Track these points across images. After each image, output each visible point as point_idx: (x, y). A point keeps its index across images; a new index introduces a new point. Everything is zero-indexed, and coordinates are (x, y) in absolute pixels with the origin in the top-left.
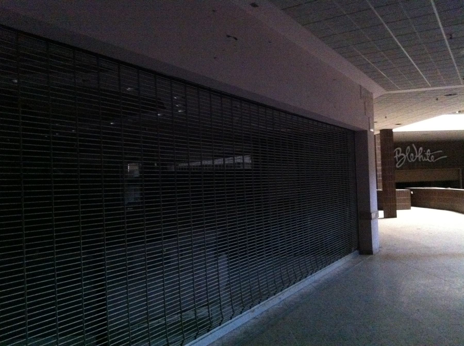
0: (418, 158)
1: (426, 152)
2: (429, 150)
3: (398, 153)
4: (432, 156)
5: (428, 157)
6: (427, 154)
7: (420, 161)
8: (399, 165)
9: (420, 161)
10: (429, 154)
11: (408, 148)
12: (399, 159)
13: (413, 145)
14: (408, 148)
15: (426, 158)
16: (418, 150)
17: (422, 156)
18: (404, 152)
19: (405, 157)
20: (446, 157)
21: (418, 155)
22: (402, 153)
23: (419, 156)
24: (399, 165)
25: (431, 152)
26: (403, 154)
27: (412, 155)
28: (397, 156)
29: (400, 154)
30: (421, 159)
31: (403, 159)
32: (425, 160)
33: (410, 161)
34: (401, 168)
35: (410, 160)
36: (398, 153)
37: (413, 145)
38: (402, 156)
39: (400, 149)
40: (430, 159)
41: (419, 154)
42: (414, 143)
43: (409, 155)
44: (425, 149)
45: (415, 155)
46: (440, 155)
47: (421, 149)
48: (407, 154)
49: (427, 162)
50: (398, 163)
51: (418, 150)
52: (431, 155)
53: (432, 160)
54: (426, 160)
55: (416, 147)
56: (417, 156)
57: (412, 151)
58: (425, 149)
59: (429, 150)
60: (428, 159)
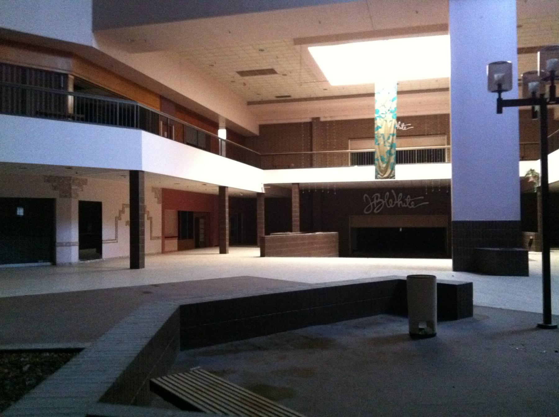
0: (397, 204)
1: (406, 198)
2: (409, 196)
4: (413, 203)
6: (407, 200)
7: (399, 206)
8: (377, 210)
9: (399, 206)
11: (388, 193)
12: (377, 204)
13: (393, 191)
14: (388, 193)
16: (397, 197)
17: (401, 202)
19: (383, 202)
23: (399, 202)
24: (377, 210)
26: (382, 200)
27: (391, 200)
28: (375, 202)
29: (379, 200)
30: (401, 204)
31: (382, 205)
32: (404, 205)
33: (388, 207)
34: (378, 214)
36: (377, 199)
37: (393, 191)
38: (381, 202)
40: (410, 204)
42: (393, 189)
43: (388, 202)
45: (394, 200)
47: (401, 194)
48: (386, 200)
50: (376, 209)
51: (397, 197)
52: (411, 201)
53: (413, 206)
55: (396, 193)
56: (396, 202)
57: (391, 196)
58: (405, 195)
60: (408, 205)
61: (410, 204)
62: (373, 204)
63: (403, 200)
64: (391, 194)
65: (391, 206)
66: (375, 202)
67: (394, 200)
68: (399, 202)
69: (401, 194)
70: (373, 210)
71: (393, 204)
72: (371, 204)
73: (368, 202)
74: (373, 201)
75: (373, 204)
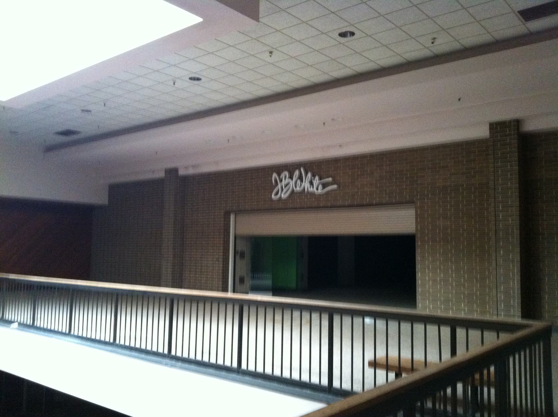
2: (317, 178)
3: (285, 179)
12: (286, 186)
26: (290, 180)
27: (299, 182)
28: (284, 183)
32: (311, 190)
35: (296, 187)
36: (285, 179)
40: (317, 189)
44: (314, 176)
45: (302, 181)
53: (320, 191)
59: (317, 178)
61: (317, 189)
63: (311, 183)
66: (284, 183)
68: (306, 185)
69: (309, 175)
72: (279, 186)
73: (277, 184)
74: (281, 181)
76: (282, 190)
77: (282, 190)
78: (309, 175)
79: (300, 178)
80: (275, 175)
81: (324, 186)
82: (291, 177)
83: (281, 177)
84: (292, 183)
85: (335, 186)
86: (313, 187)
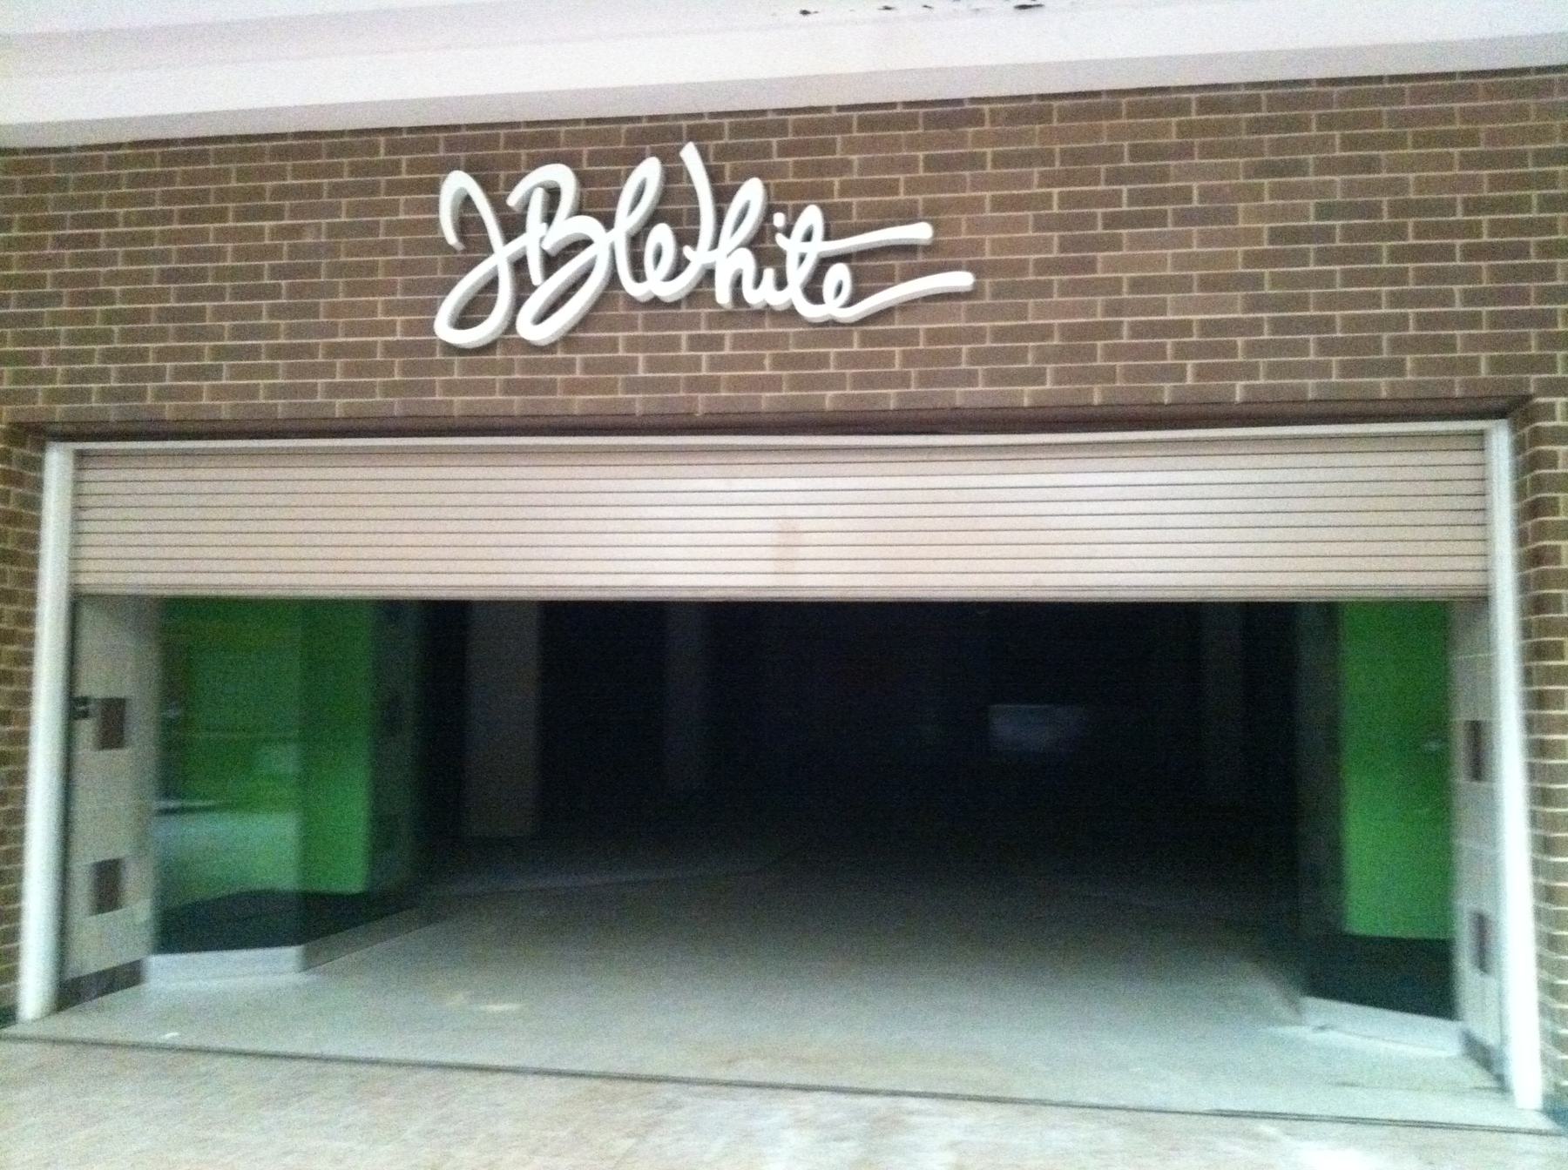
0: (709, 275)
2: (812, 216)
4: (839, 273)
5: (798, 275)
6: (790, 246)
7: (723, 295)
8: (542, 318)
9: (723, 295)
10: (820, 246)
11: (649, 171)
12: (552, 263)
13: (690, 155)
15: (781, 283)
16: (723, 197)
17: (746, 262)
18: (597, 203)
20: (961, 280)
21: (715, 244)
22: (579, 211)
23: (726, 257)
24: (542, 318)
25: (827, 237)
26: (588, 226)
27: (662, 235)
28: (537, 239)
29: (568, 226)
30: (738, 282)
35: (639, 275)
36: (549, 218)
37: (690, 155)
39: (561, 175)
40: (813, 292)
41: (729, 240)
42: (701, 129)
43: (637, 240)
44: (783, 200)
45: (686, 237)
46: (912, 260)
49: (791, 313)
51: (723, 197)
52: (824, 263)
53: (833, 308)
54: (778, 299)
55: (714, 175)
56: (698, 257)
59: (812, 216)
60: (793, 294)
61: (813, 292)
62: (520, 265)
63: (764, 249)
64: (674, 174)
65: (657, 285)
66: (537, 239)
67: (686, 237)
69: (752, 193)
70: (518, 302)
71: (680, 265)
72: (501, 256)
73: (475, 243)
74: (513, 226)
75: (520, 265)
76: (524, 288)
77: (524, 288)
78: (752, 193)
79: (674, 208)
80: (458, 183)
81: (871, 269)
82: (597, 203)
83: (513, 200)
84: (607, 245)
85: (961, 280)
86: (781, 283)
